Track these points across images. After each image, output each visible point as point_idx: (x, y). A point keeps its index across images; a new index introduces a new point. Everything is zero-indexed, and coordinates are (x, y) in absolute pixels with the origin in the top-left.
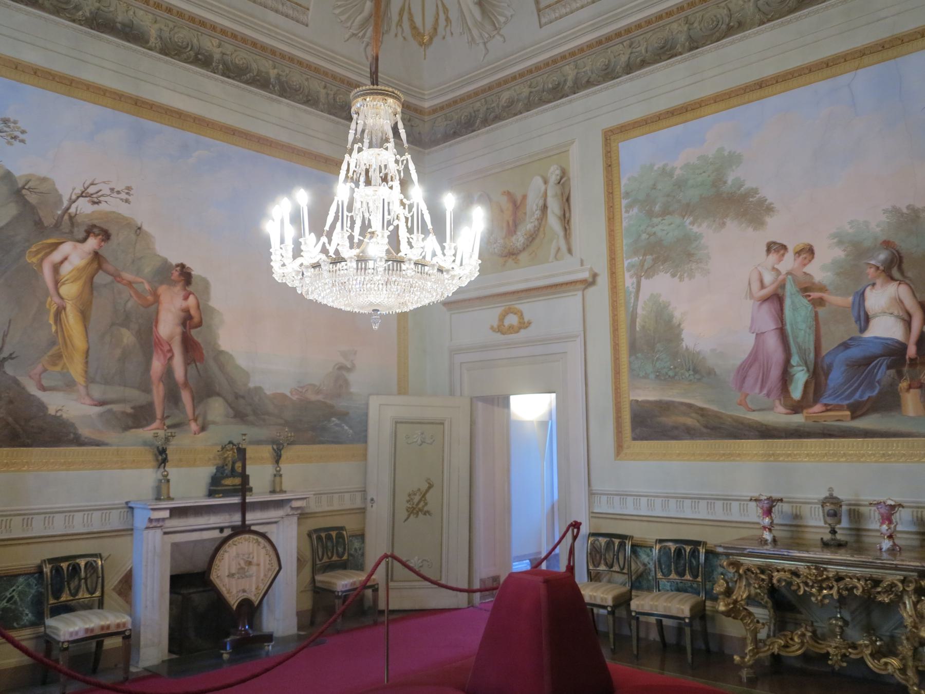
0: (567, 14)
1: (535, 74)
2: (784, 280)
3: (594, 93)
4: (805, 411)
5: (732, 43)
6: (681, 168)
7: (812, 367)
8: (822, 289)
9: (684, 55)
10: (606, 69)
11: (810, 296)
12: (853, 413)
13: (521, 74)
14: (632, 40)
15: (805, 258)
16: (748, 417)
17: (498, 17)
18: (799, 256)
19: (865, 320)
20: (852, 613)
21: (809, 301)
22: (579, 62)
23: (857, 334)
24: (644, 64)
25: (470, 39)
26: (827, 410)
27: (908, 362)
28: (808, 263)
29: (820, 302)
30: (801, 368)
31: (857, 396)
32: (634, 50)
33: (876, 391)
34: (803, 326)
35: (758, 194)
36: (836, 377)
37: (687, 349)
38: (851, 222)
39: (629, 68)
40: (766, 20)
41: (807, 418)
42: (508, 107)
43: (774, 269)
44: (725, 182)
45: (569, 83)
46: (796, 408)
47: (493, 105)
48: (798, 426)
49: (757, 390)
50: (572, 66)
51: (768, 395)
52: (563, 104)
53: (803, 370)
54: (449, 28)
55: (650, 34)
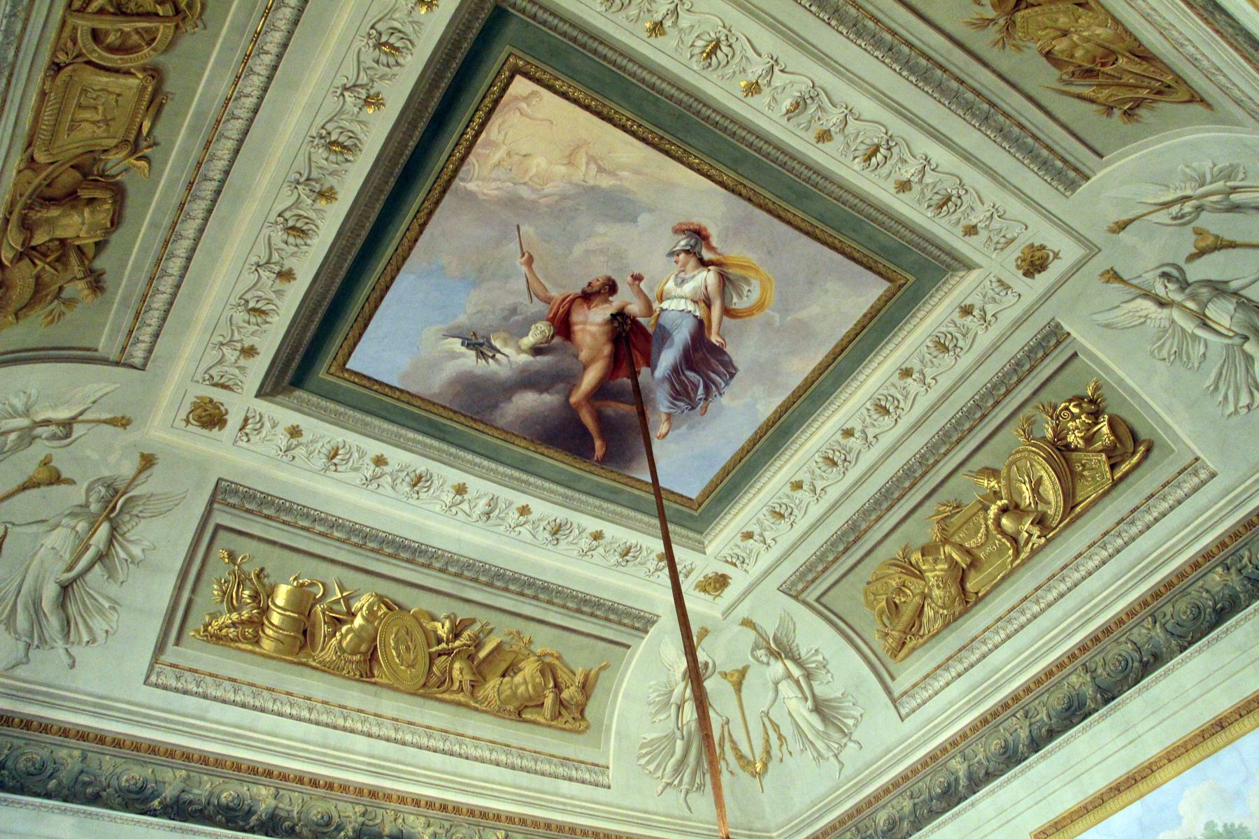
0: (930, 697)
1: (914, 780)
3: (1001, 786)
5: (1157, 680)
9: (1100, 712)
10: (1005, 752)
13: (895, 784)
14: (1027, 708)
17: (845, 720)
22: (966, 751)
24: (1052, 734)
25: (816, 755)
32: (1033, 720)
39: (1036, 744)
40: (1186, 644)
42: (890, 830)
45: (963, 782)
47: (869, 833)
50: (958, 759)
52: (965, 810)
54: (784, 746)
55: (1046, 695)
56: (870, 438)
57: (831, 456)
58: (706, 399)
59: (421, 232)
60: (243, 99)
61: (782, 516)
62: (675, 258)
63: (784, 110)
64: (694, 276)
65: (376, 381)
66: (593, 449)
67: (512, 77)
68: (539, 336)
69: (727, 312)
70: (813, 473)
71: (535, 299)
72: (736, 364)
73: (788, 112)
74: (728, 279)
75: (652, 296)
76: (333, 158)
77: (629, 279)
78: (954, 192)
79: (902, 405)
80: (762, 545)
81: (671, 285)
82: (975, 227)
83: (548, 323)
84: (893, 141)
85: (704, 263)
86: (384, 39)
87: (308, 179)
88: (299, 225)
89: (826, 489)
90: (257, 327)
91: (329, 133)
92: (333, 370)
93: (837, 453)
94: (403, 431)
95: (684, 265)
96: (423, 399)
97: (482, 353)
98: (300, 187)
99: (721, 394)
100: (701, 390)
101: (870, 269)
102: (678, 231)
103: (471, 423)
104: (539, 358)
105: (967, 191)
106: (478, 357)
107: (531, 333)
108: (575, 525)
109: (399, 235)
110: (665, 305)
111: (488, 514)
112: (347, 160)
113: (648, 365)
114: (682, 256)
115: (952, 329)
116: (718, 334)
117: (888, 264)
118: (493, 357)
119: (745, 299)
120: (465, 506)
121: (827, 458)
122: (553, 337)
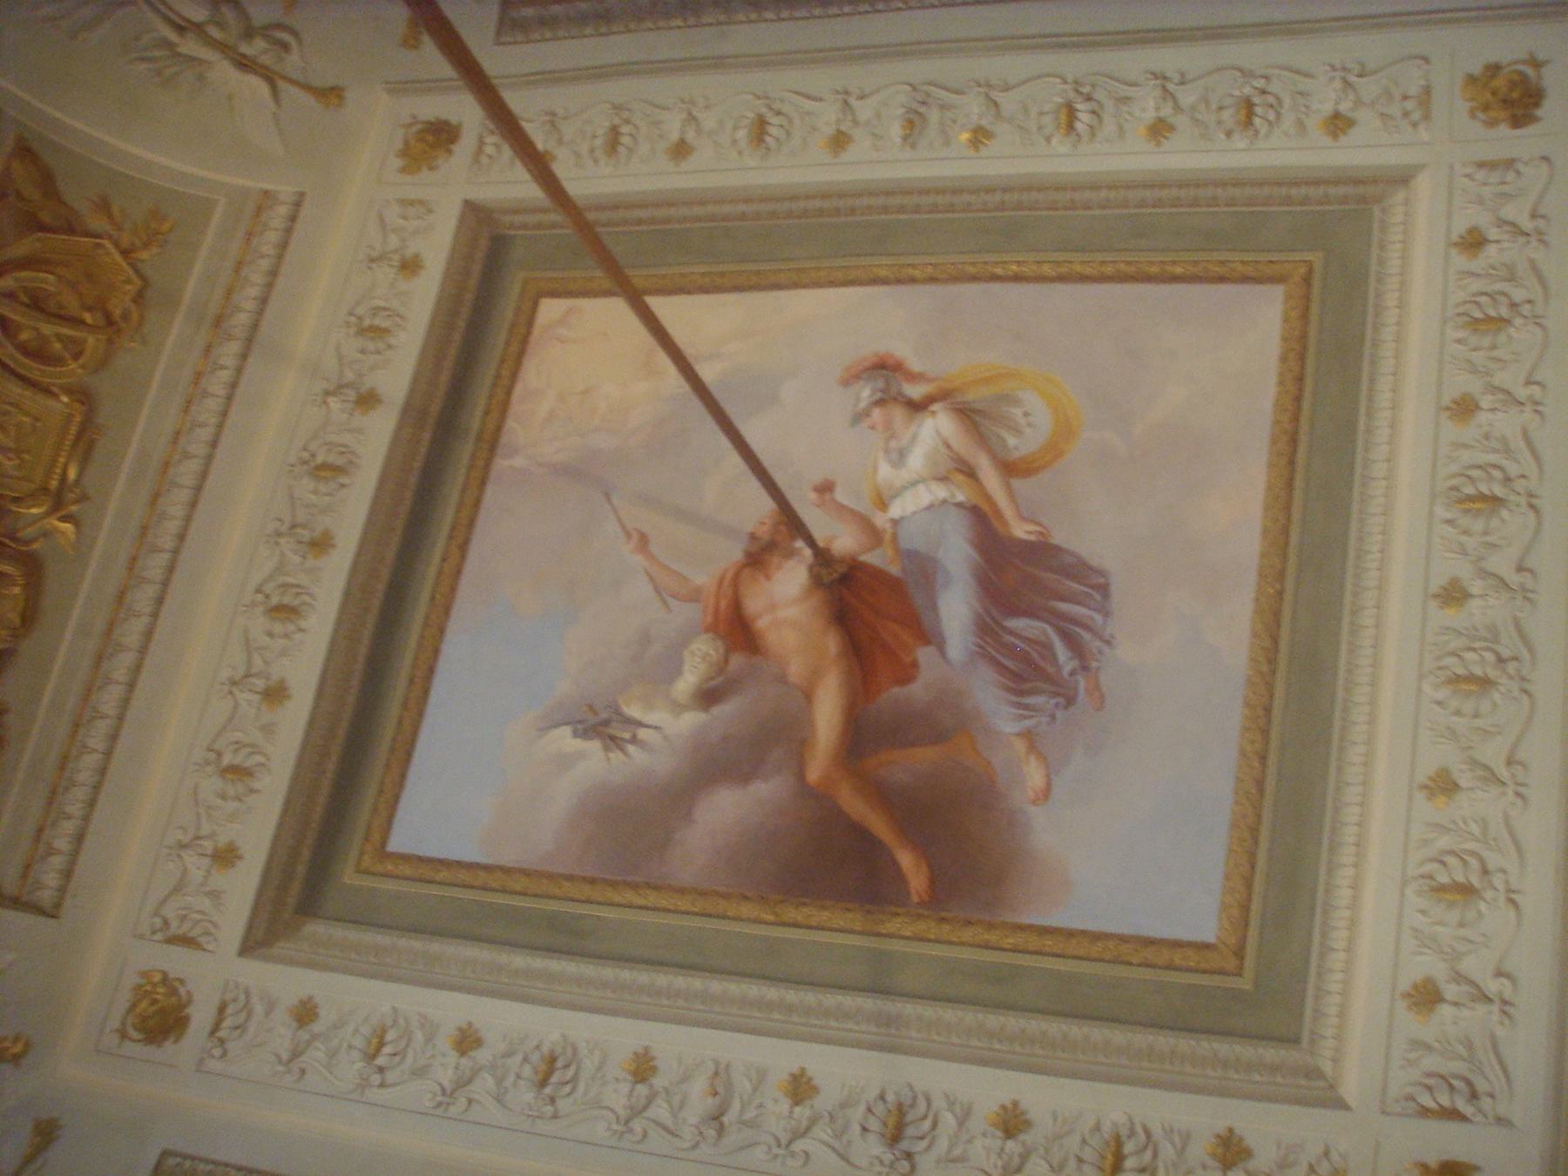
56: (1514, 579)
57: (1461, 671)
58: (1085, 668)
59: (463, 557)
60: (198, 430)
61: (1466, 891)
62: (867, 422)
63: (898, 140)
64: (914, 438)
65: (440, 861)
66: (900, 877)
67: (535, 305)
68: (702, 667)
69: (1011, 469)
70: (1452, 734)
71: (672, 602)
72: (1095, 562)
73: (905, 138)
74: (974, 411)
75: (864, 506)
76: (323, 488)
77: (813, 496)
78: (1247, 90)
79: (1513, 469)
80: (1481, 1009)
81: (885, 471)
82: (1337, 116)
83: (710, 635)
84: (1082, 85)
85: (917, 407)
86: (367, 323)
87: (294, 526)
88: (287, 600)
89: (1521, 755)
90: (235, 804)
91: (313, 456)
92: (367, 862)
93: (1470, 656)
94: (504, 957)
95: (888, 425)
96: (526, 873)
97: (613, 738)
98: (282, 541)
99: (1108, 643)
100: (1061, 652)
101: (1222, 279)
102: (852, 377)
103: (630, 896)
104: (717, 710)
105: (1266, 77)
106: (607, 749)
107: (686, 667)
108: (939, 1103)
109: (432, 572)
110: (895, 511)
111: (716, 1117)
112: (343, 486)
113: (928, 642)
114: (877, 413)
115: (1476, 285)
116: (1023, 519)
117: (1250, 257)
118: (634, 740)
119: (1028, 431)
120: (660, 1110)
121: (1456, 680)
122: (726, 661)
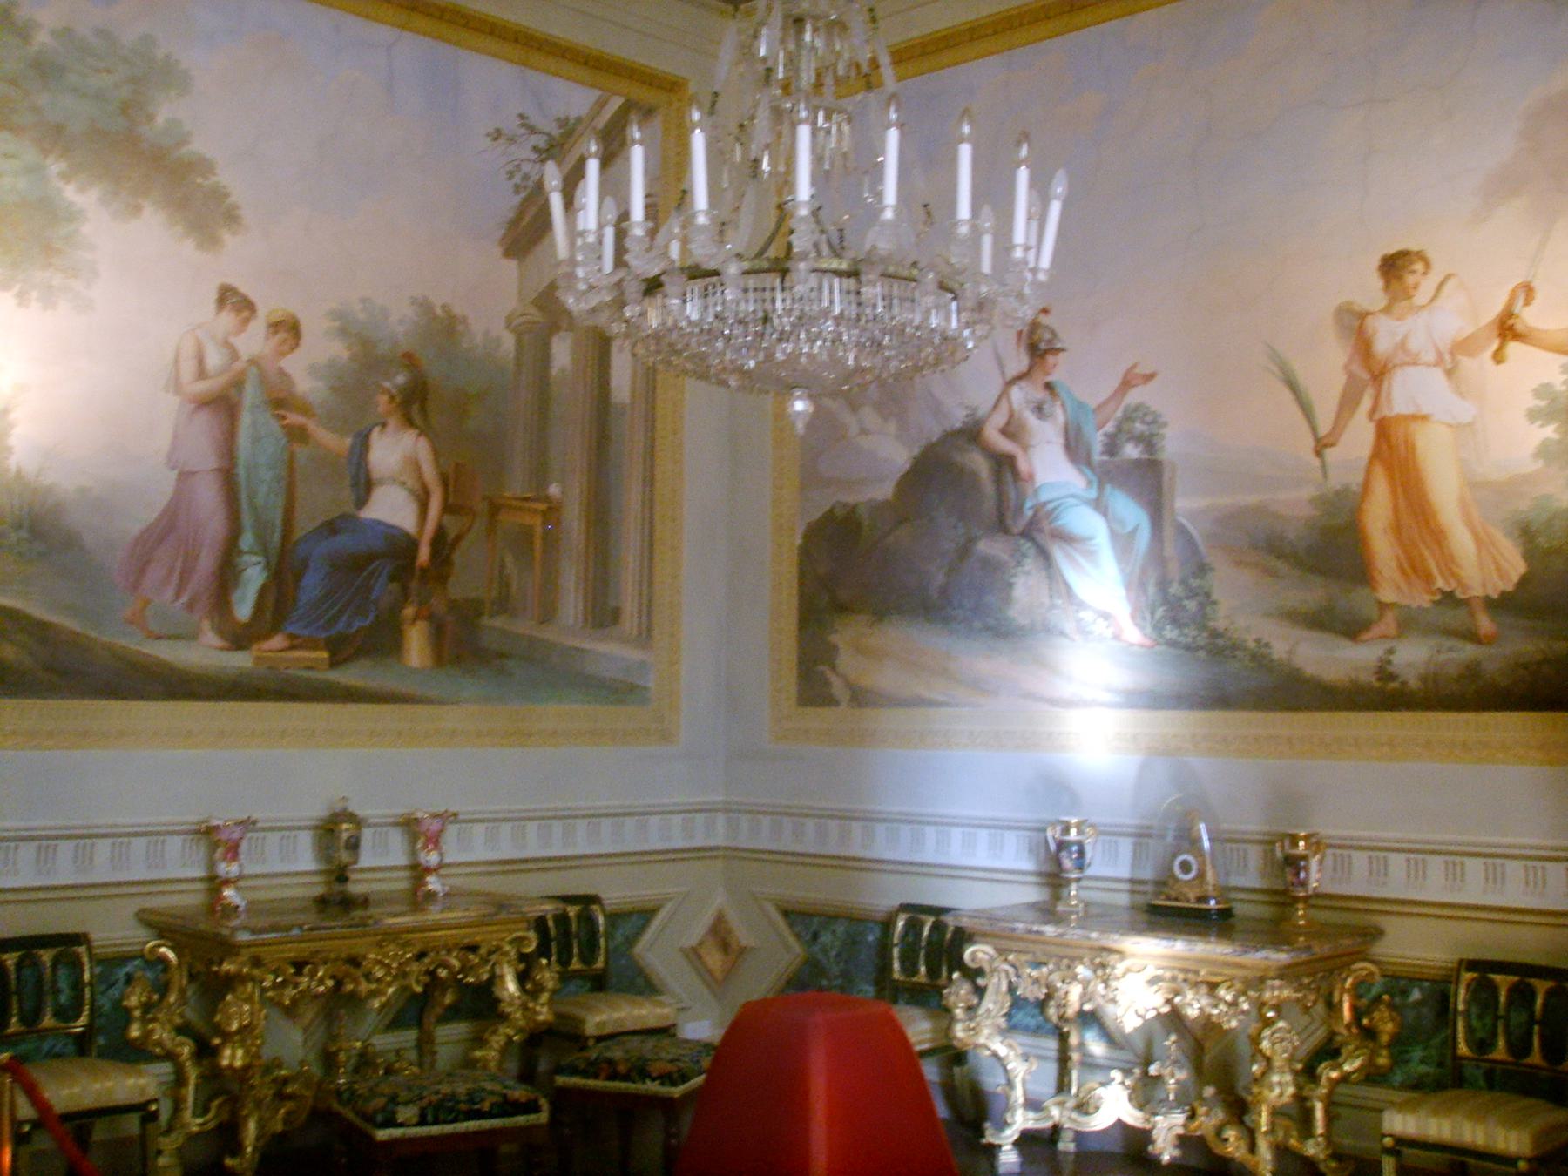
2: (243, 372)
4: (255, 647)
6: (54, 33)
7: (274, 561)
8: (305, 410)
11: (284, 418)
12: (333, 654)
15: (285, 341)
16: (146, 650)
18: (276, 332)
19: (364, 486)
20: (305, 1030)
21: (284, 427)
23: (349, 508)
26: (292, 648)
27: (417, 573)
28: (288, 353)
29: (298, 435)
30: (255, 559)
31: (341, 626)
33: (371, 618)
34: (267, 475)
35: (214, 174)
36: (312, 585)
37: (19, 472)
38: (363, 300)
41: (258, 659)
43: (227, 344)
44: (150, 118)
46: (240, 639)
48: (241, 674)
49: (170, 593)
51: (190, 606)
53: (259, 563)
